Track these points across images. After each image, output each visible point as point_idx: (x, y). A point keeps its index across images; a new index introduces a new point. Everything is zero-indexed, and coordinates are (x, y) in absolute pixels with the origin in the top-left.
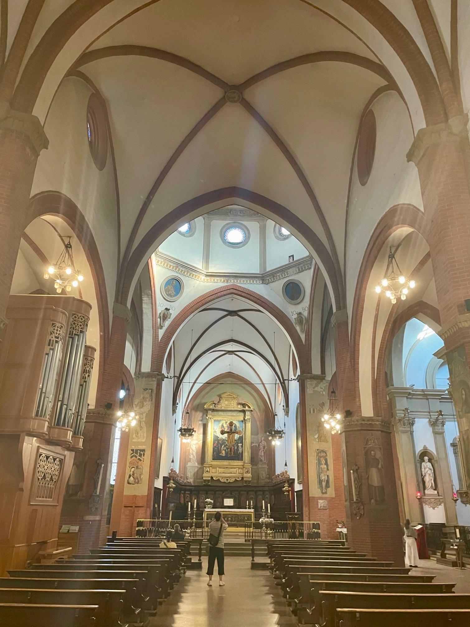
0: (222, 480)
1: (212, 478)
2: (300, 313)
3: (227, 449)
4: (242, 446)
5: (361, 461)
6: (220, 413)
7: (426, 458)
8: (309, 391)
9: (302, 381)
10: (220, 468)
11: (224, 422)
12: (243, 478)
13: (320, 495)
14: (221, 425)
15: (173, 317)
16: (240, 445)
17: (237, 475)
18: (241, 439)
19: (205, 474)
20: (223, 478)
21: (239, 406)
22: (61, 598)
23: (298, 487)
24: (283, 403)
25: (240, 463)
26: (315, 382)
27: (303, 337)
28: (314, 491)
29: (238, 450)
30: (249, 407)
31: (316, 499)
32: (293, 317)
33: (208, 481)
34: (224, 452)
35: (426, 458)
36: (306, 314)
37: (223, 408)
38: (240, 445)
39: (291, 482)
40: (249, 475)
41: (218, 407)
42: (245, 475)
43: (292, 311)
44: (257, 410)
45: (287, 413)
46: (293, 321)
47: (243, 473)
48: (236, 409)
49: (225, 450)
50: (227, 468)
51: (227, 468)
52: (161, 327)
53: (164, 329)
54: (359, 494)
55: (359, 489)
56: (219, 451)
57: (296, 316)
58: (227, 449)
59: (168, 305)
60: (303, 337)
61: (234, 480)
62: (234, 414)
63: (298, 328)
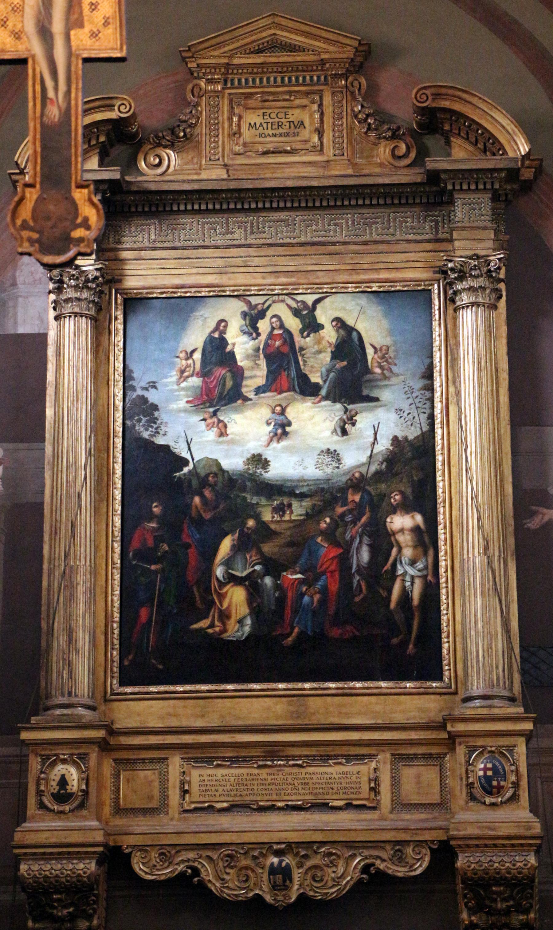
0: (224, 883)
1: (115, 858)
3: (273, 567)
4: (426, 538)
6: (192, 227)
10: (200, 755)
11: (232, 313)
12: (444, 853)
14: (195, 337)
16: (401, 522)
17: (381, 822)
18: (412, 466)
19: (41, 828)
20: (231, 853)
21: (383, 151)
25: (406, 704)
29: (380, 573)
30: (489, 144)
33: (78, 891)
34: (237, 597)
37: (213, 175)
38: (401, 522)
40: (517, 817)
41: (166, 168)
42: (470, 819)
47: (442, 805)
48: (339, 173)
49: (251, 584)
50: (273, 752)
51: (273, 752)
56: (199, 596)
58: (273, 567)
61: (347, 872)
62: (339, 227)
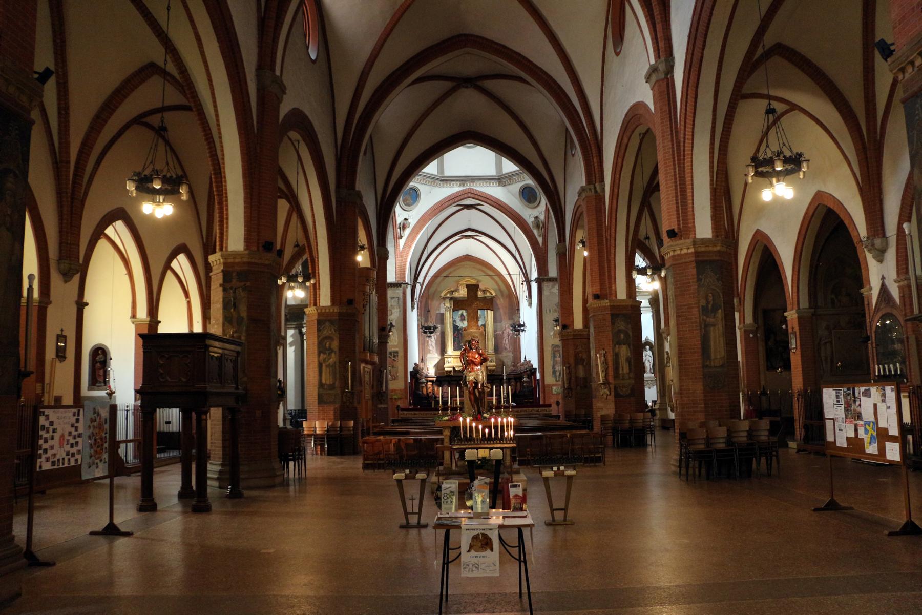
2: (537, 218)
5: (572, 361)
7: (648, 347)
8: (546, 293)
9: (539, 281)
13: (555, 383)
15: (412, 226)
22: (407, 433)
23: (538, 376)
24: (526, 293)
26: (551, 284)
27: (540, 240)
28: (549, 380)
31: (550, 386)
32: (530, 221)
35: (648, 347)
36: (542, 217)
39: (532, 372)
43: (529, 214)
44: (499, 295)
45: (530, 305)
46: (531, 224)
52: (401, 237)
53: (404, 239)
54: (570, 383)
55: (570, 379)
57: (533, 219)
59: (406, 215)
60: (540, 240)
63: (535, 232)
